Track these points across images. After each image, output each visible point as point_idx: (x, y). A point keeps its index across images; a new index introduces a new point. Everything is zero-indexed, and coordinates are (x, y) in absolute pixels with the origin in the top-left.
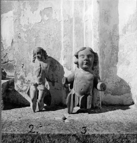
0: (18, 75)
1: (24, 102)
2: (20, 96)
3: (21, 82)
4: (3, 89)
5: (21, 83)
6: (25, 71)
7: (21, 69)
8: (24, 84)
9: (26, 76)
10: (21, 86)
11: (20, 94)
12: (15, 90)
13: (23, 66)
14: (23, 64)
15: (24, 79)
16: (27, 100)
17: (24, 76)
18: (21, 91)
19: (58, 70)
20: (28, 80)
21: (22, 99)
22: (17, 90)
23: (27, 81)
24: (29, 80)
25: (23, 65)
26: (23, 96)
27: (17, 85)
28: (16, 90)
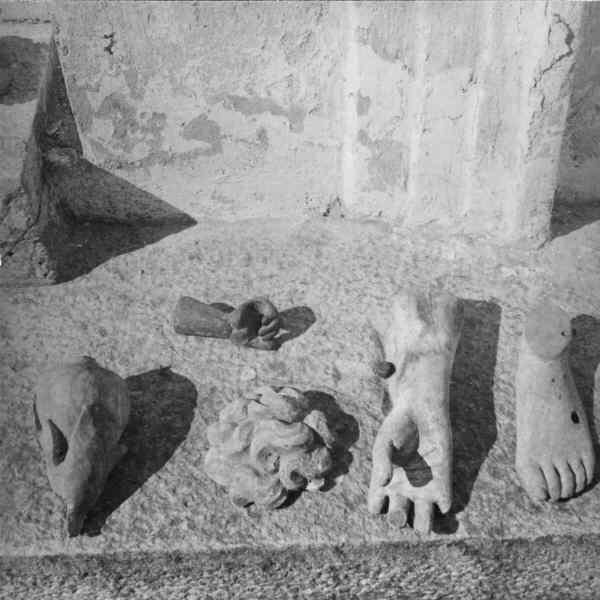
0: (89, 93)
1: (145, 207)
2: (123, 188)
3: (114, 123)
4: (29, 198)
5: (115, 132)
6: (124, 67)
7: (105, 62)
8: (133, 132)
9: (139, 96)
10: (120, 141)
11: (117, 179)
12: (90, 167)
13: (111, 46)
14: (111, 36)
15: (128, 111)
16: (163, 198)
17: (124, 97)
18: (120, 167)
19: (324, 54)
20: (155, 114)
21: (133, 199)
22: (102, 161)
23: (149, 116)
24: (160, 111)
25: (109, 41)
26: (139, 185)
27: (92, 142)
28: (95, 163)
